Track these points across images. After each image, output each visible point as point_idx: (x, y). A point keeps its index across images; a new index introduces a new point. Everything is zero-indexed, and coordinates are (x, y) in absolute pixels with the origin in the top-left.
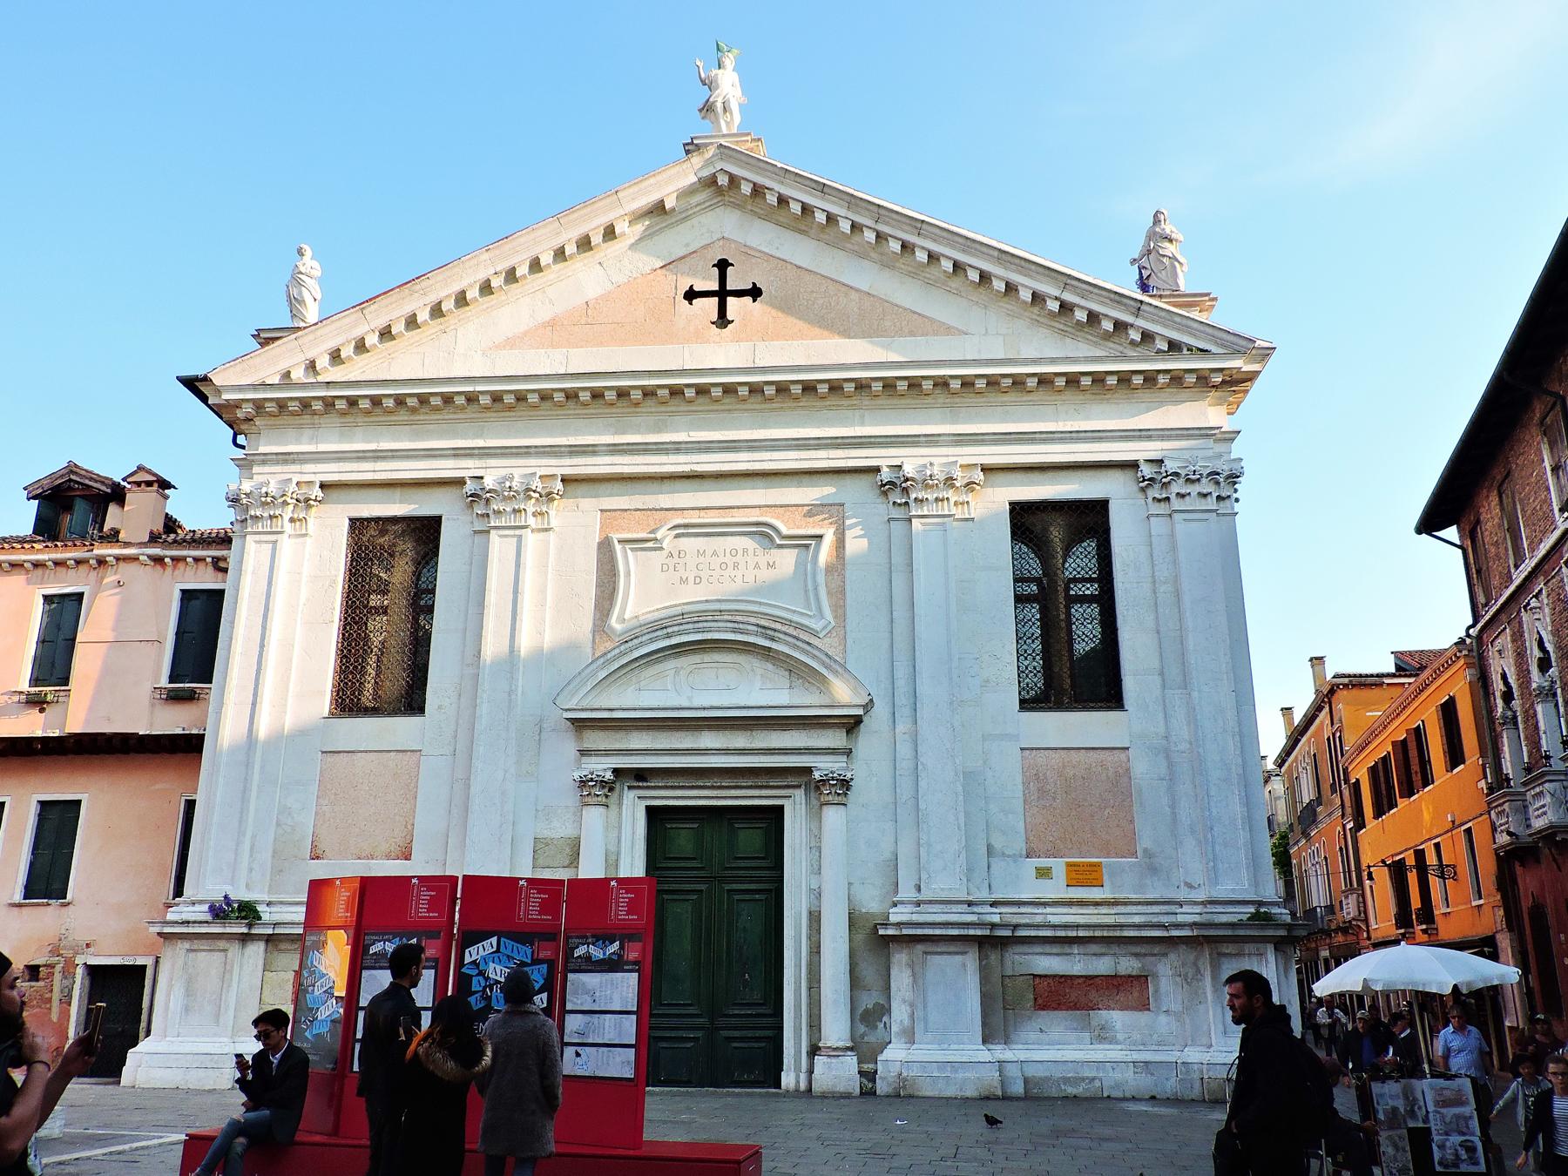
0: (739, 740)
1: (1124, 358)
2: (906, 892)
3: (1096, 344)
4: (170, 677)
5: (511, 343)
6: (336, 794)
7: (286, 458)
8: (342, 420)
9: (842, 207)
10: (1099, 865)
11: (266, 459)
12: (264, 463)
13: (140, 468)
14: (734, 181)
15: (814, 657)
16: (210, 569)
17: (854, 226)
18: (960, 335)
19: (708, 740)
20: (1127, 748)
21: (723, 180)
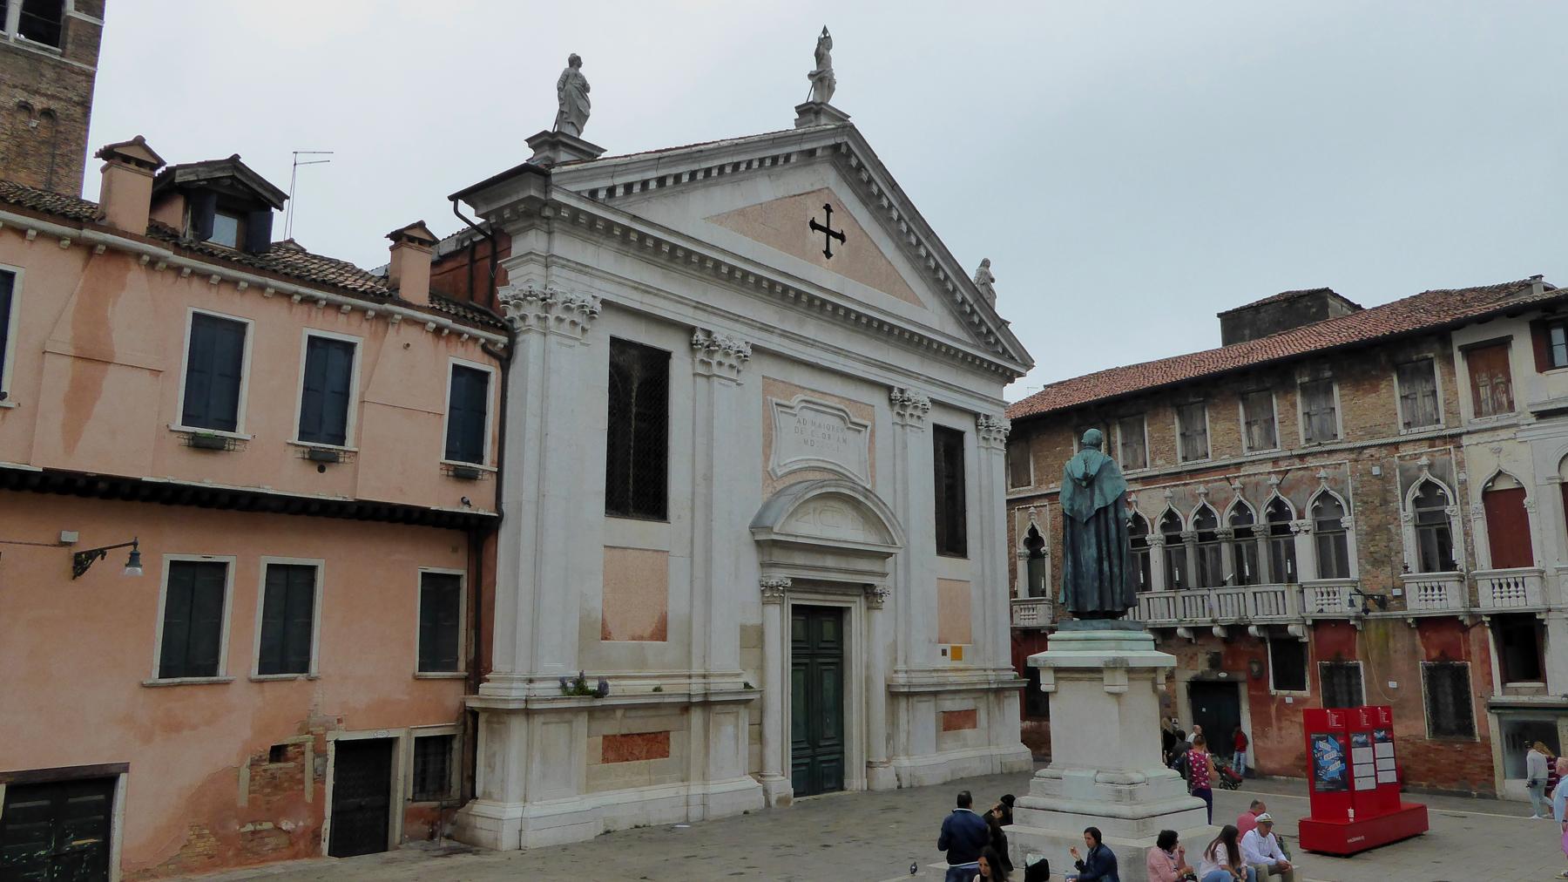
0: (843, 563)
1: (977, 347)
2: (901, 666)
3: (970, 336)
4: (447, 452)
5: (720, 219)
6: (615, 584)
7: (582, 268)
8: (620, 248)
9: (897, 201)
10: (960, 648)
11: (567, 264)
12: (563, 266)
13: (421, 225)
14: (850, 152)
15: (884, 513)
16: (479, 349)
17: (900, 218)
18: (919, 306)
19: (830, 562)
20: (968, 581)
21: (844, 149)
